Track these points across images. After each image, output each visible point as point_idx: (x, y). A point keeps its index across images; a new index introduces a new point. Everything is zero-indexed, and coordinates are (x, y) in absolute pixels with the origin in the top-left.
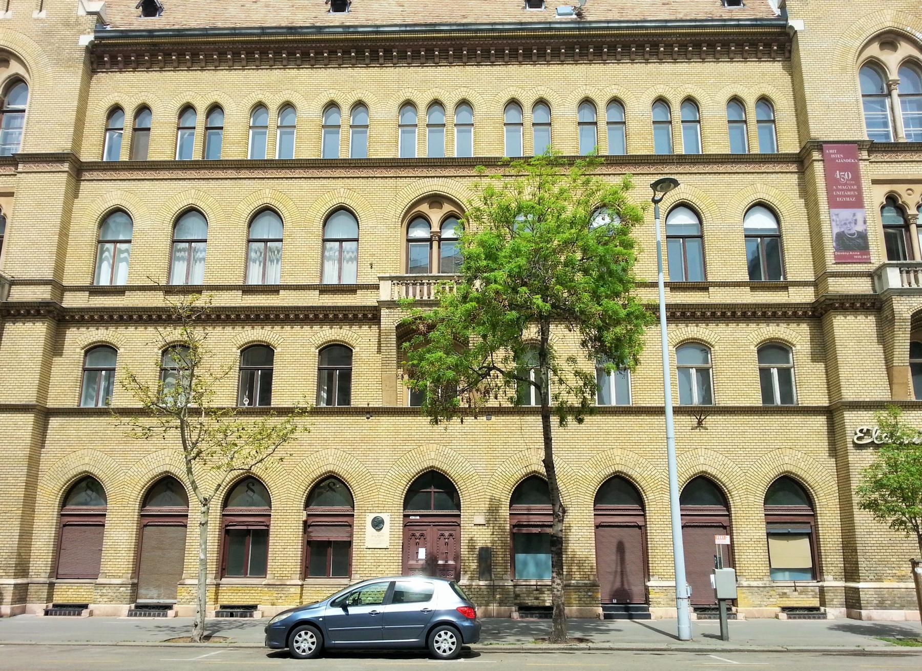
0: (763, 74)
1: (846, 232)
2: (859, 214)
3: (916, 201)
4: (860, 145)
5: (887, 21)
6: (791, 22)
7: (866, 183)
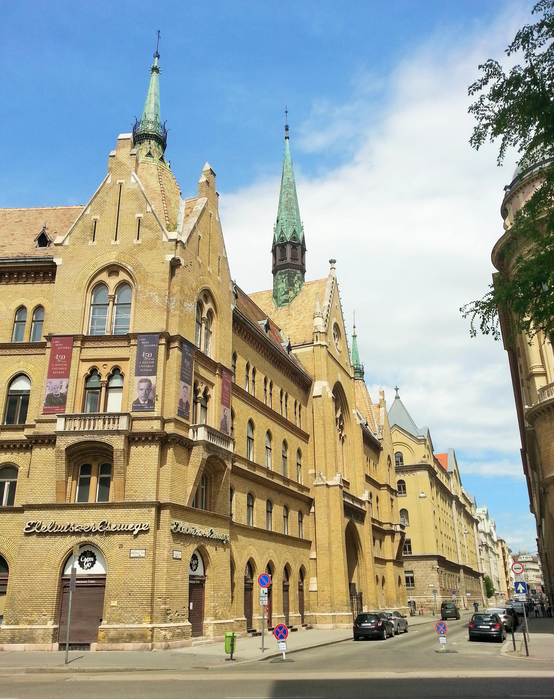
0: (42, 291)
2: (65, 381)
4: (75, 338)
5: (112, 258)
6: (54, 260)
7: (74, 362)
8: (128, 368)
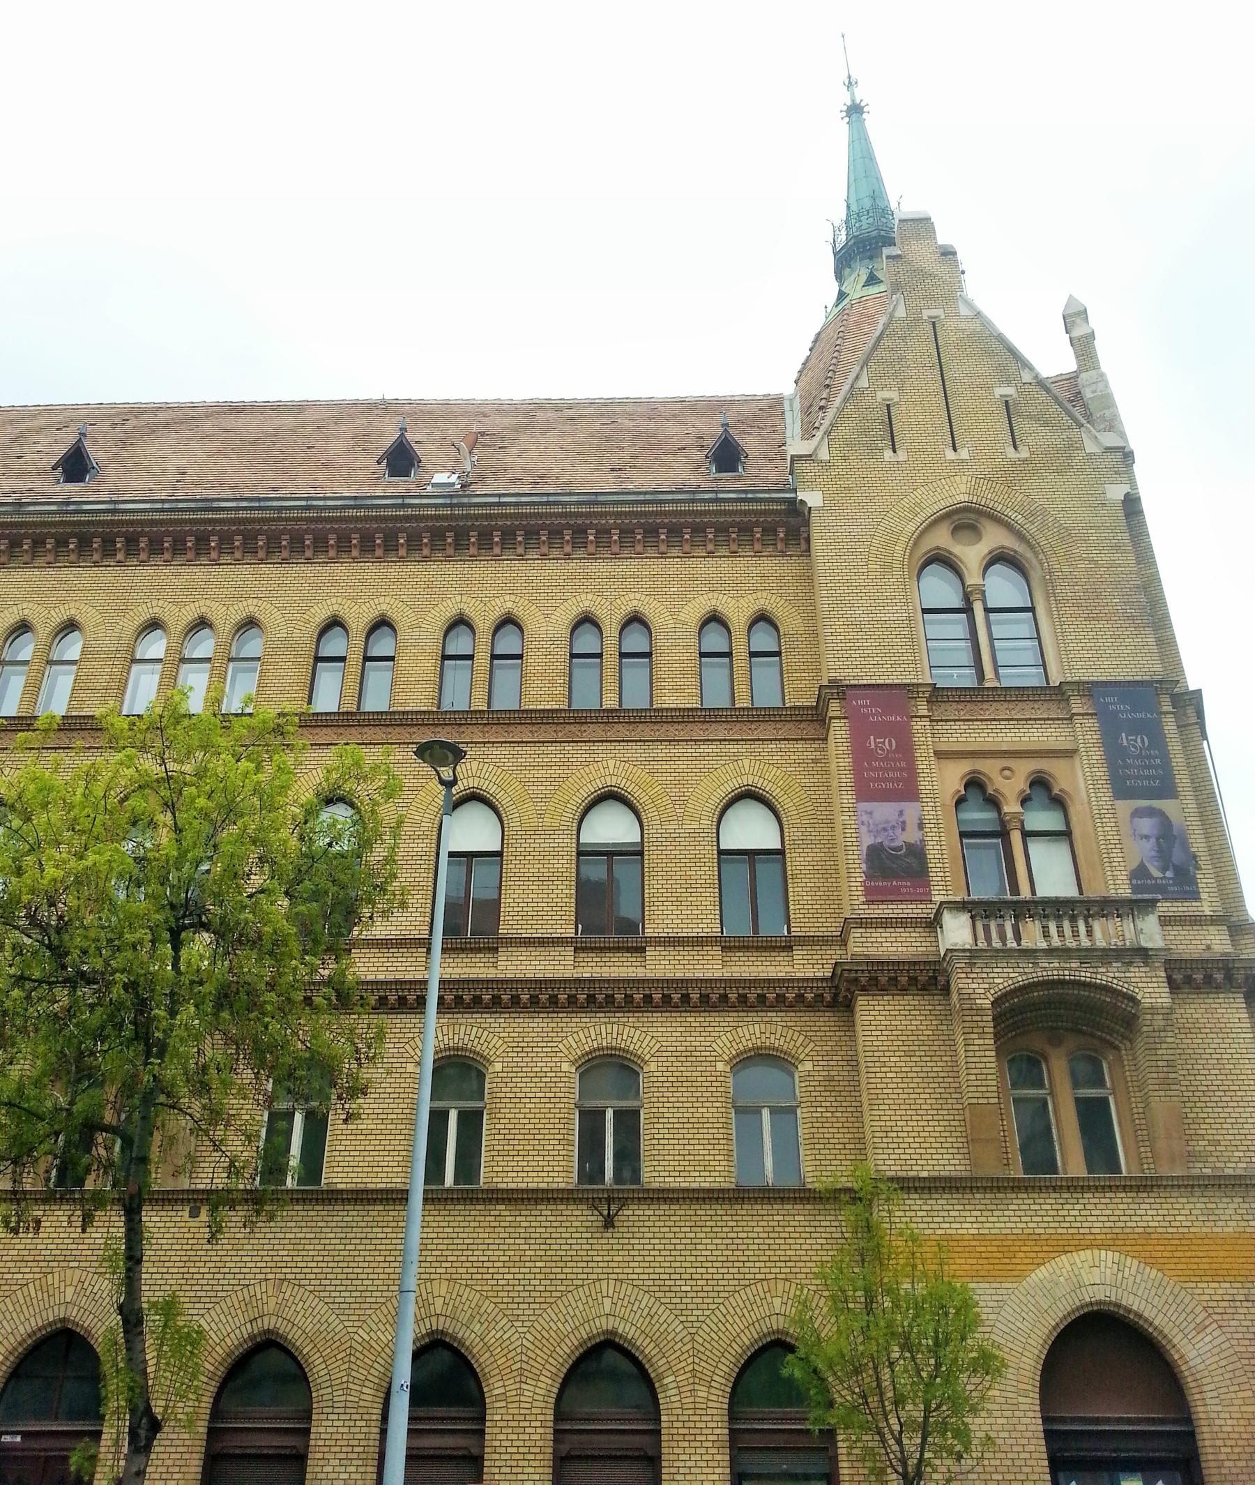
1: (886, 843)
2: (911, 811)
3: (1018, 789)
5: (959, 491)
6: (801, 495)
7: (924, 758)
8: (1084, 780)
